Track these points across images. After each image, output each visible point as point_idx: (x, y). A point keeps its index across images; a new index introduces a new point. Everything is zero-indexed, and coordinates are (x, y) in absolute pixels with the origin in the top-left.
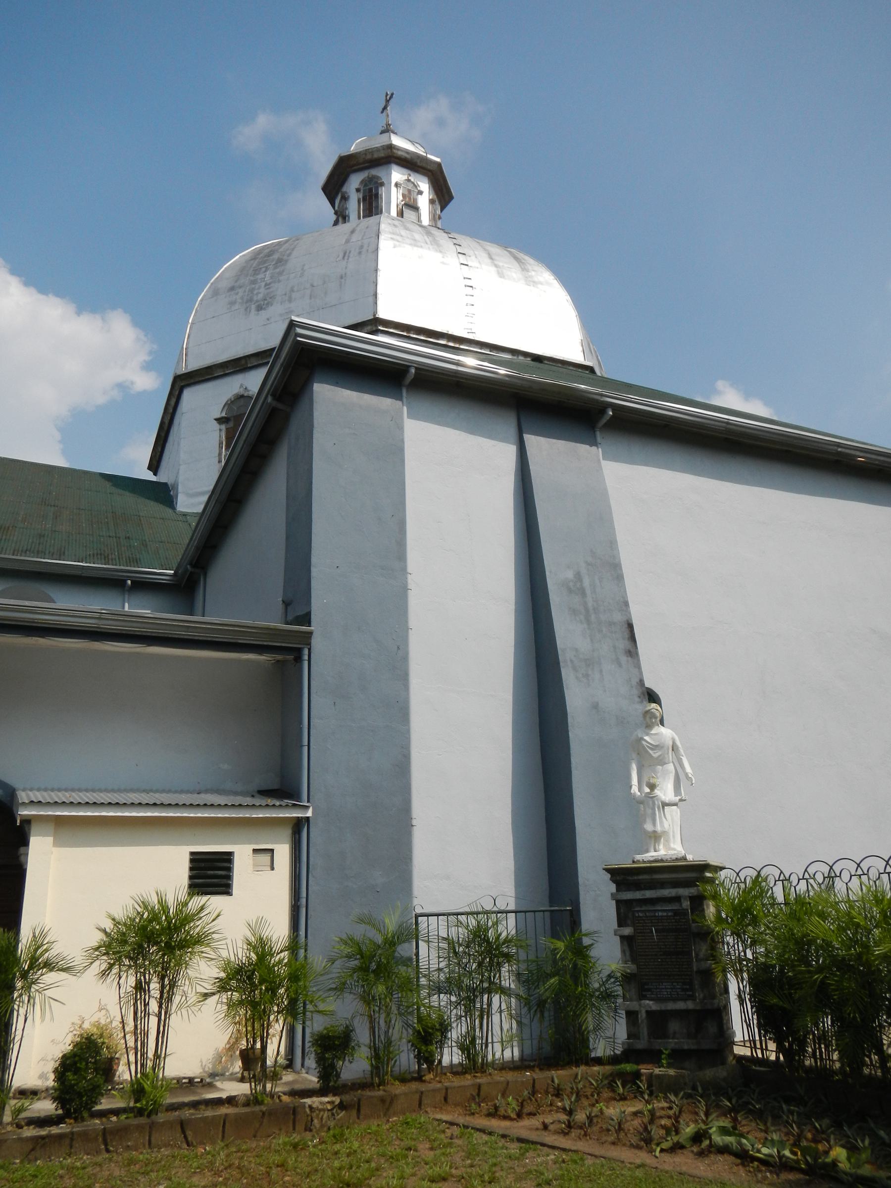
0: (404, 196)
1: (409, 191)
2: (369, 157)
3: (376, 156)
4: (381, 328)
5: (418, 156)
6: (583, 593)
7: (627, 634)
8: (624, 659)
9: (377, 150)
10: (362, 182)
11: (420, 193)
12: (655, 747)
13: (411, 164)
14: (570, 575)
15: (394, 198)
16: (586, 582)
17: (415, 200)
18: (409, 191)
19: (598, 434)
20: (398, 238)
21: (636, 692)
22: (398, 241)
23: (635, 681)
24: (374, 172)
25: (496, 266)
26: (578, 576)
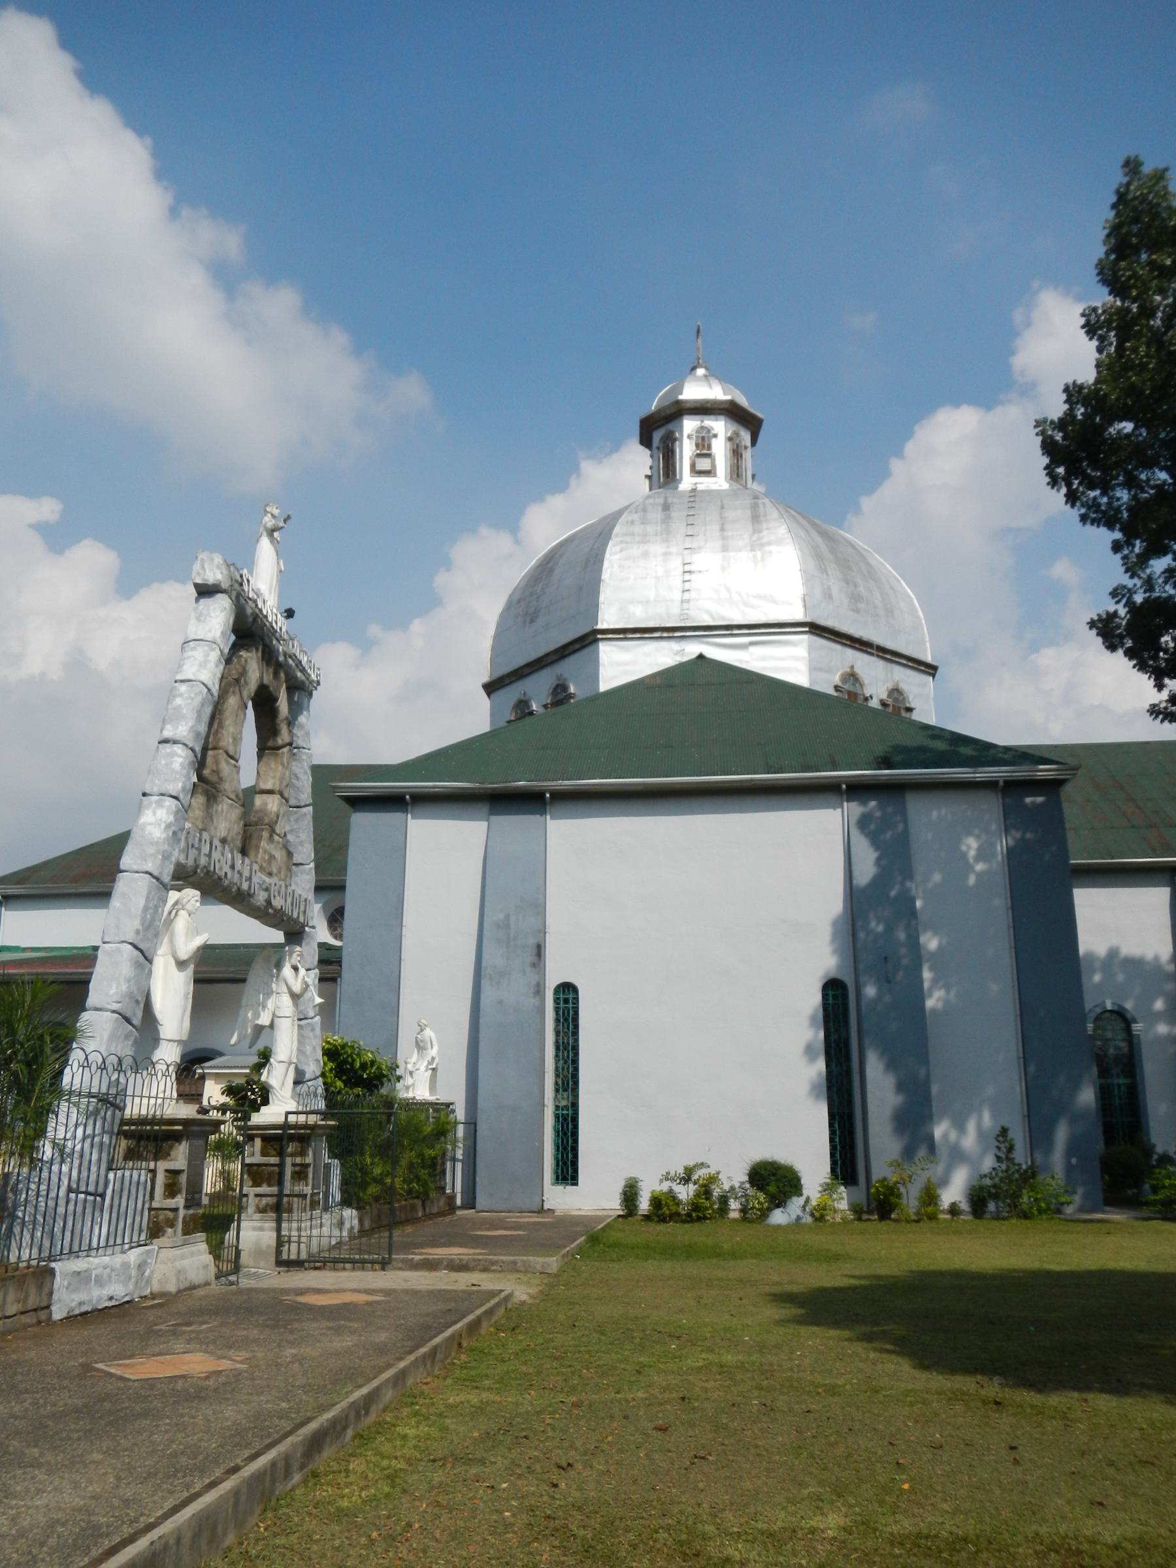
0: (697, 446)
1: (703, 438)
2: (663, 414)
3: (668, 412)
4: (599, 636)
5: (707, 401)
6: (507, 926)
7: (535, 952)
8: (528, 969)
9: (668, 407)
10: (661, 439)
11: (715, 436)
12: (422, 1041)
13: (704, 409)
14: (501, 916)
15: (686, 450)
16: (513, 919)
17: (709, 447)
18: (703, 438)
19: (548, 808)
20: (628, 539)
21: (532, 990)
22: (627, 543)
23: (534, 983)
24: (670, 426)
25: (724, 538)
26: (507, 917)
